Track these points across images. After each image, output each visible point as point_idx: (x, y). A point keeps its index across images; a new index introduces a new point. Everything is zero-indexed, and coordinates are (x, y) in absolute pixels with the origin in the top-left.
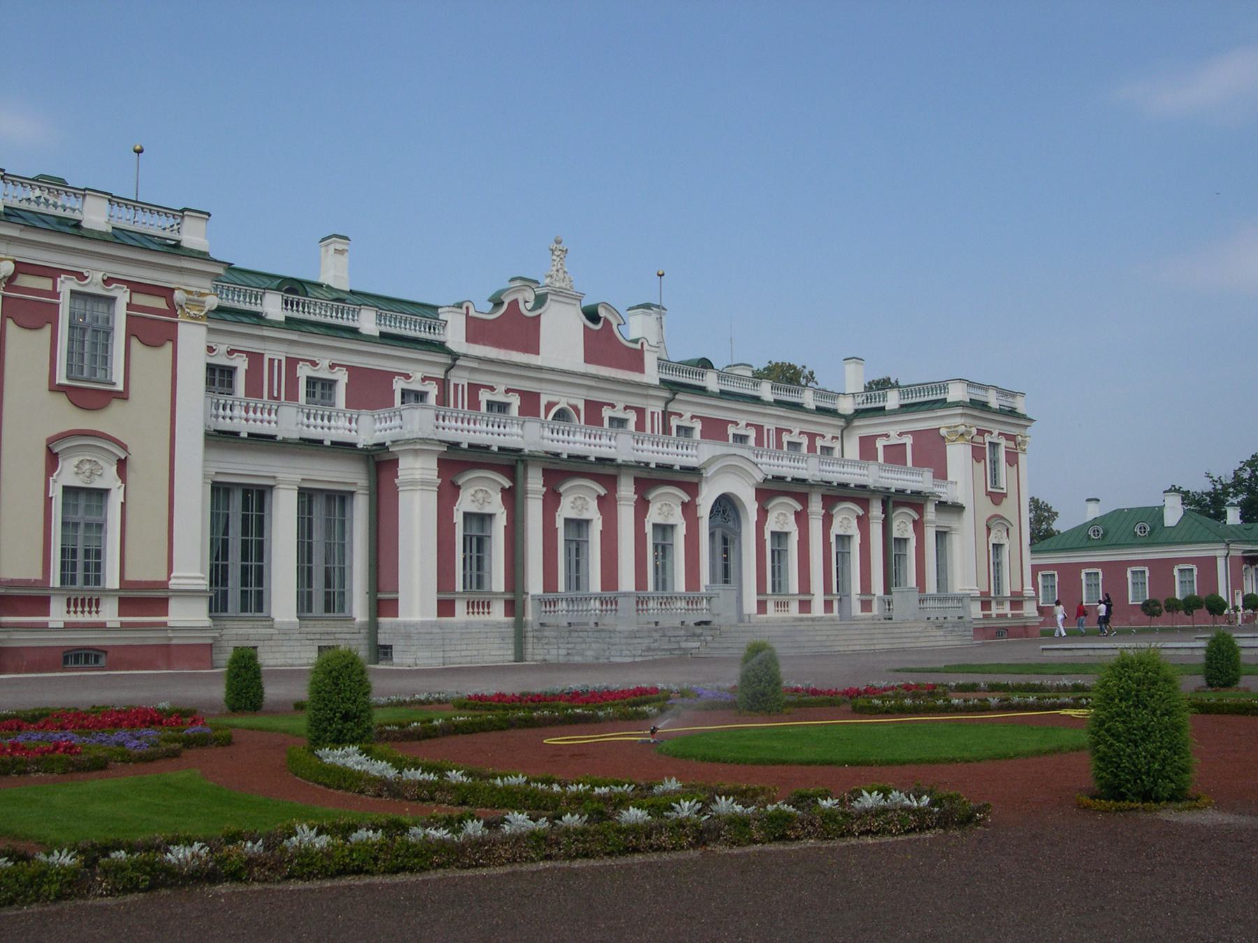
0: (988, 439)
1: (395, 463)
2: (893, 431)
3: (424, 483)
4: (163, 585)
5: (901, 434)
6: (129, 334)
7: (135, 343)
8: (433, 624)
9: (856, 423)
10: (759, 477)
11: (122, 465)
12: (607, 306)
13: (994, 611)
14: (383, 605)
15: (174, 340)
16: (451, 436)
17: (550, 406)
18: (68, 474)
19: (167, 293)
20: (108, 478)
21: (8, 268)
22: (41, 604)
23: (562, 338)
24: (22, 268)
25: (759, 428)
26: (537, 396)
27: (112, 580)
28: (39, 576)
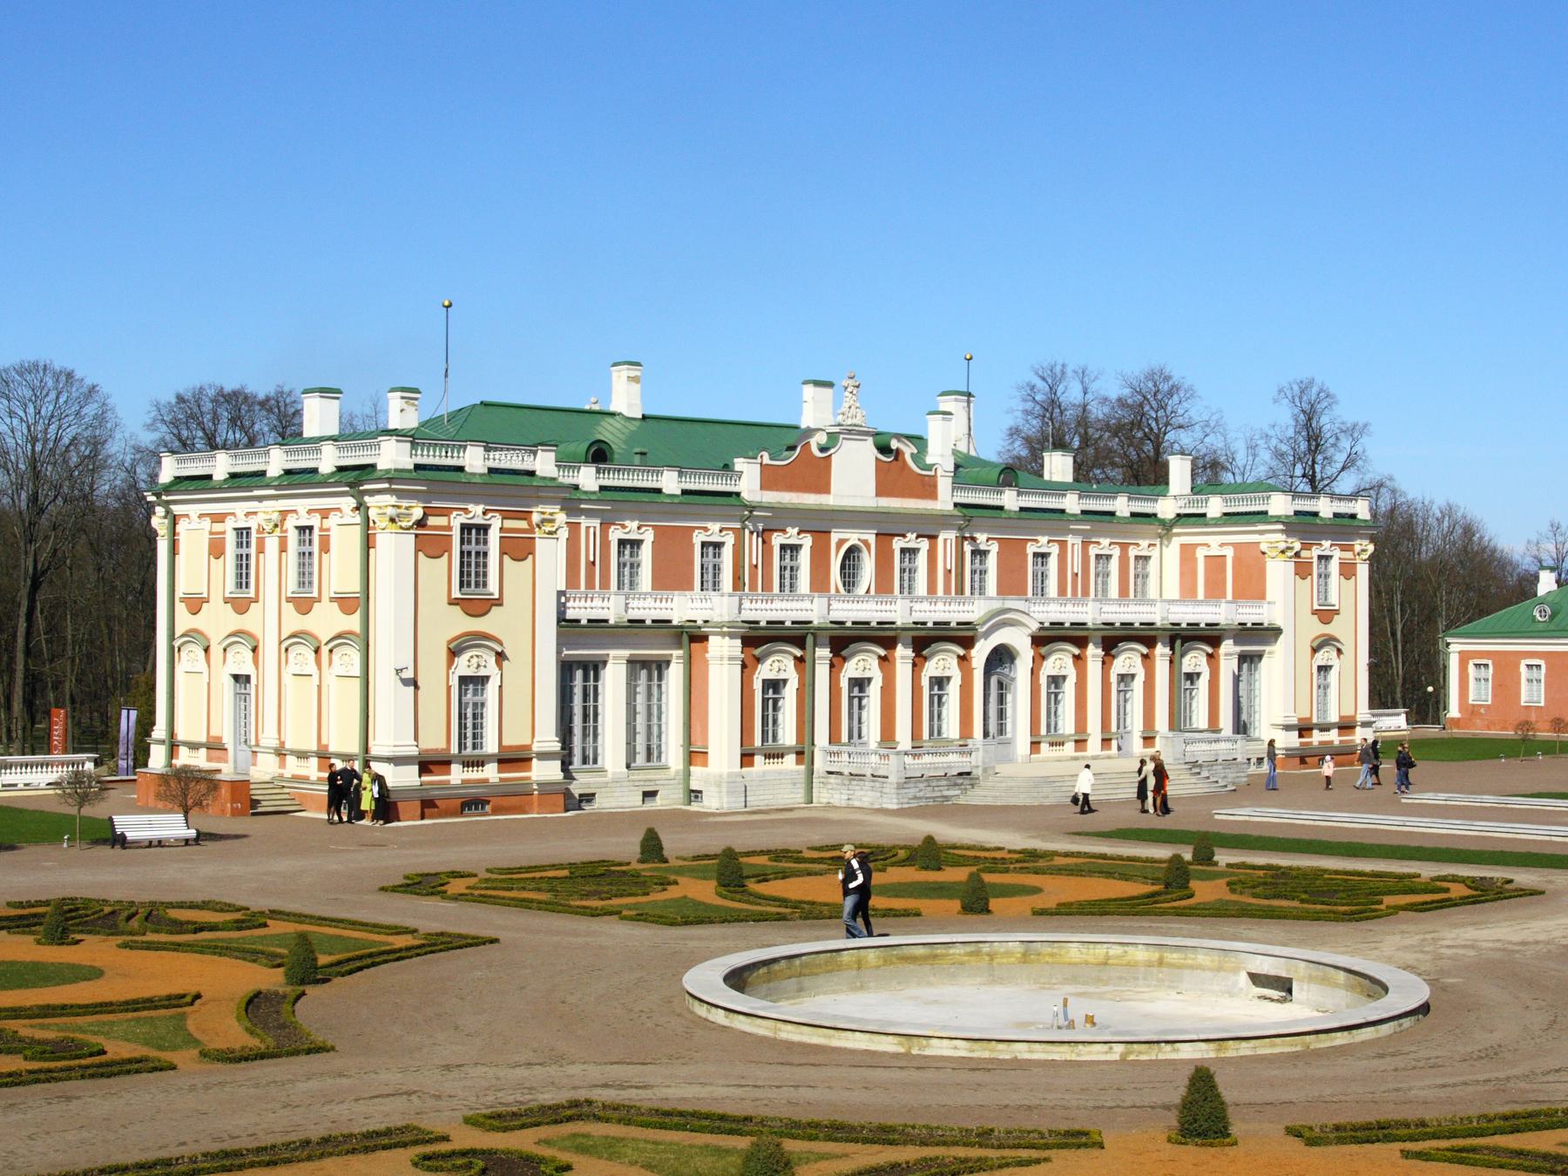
1: (704, 638)
2: (1214, 541)
3: (730, 659)
4: (528, 748)
5: (1222, 545)
6: (502, 553)
7: (506, 557)
8: (737, 775)
10: (1035, 626)
11: (501, 656)
14: (694, 755)
15: (532, 553)
16: (748, 615)
17: (841, 542)
28: (443, 745)
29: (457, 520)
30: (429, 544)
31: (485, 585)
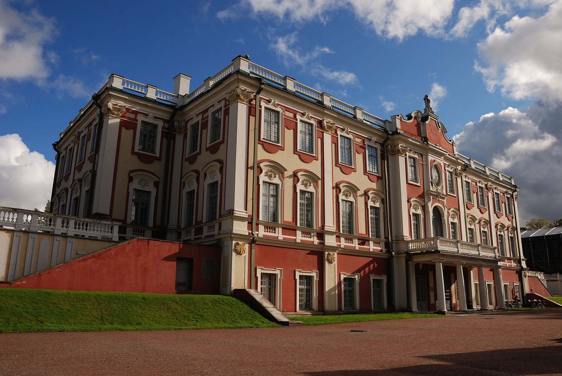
18: (135, 185)
27: (151, 224)
31: (153, 151)
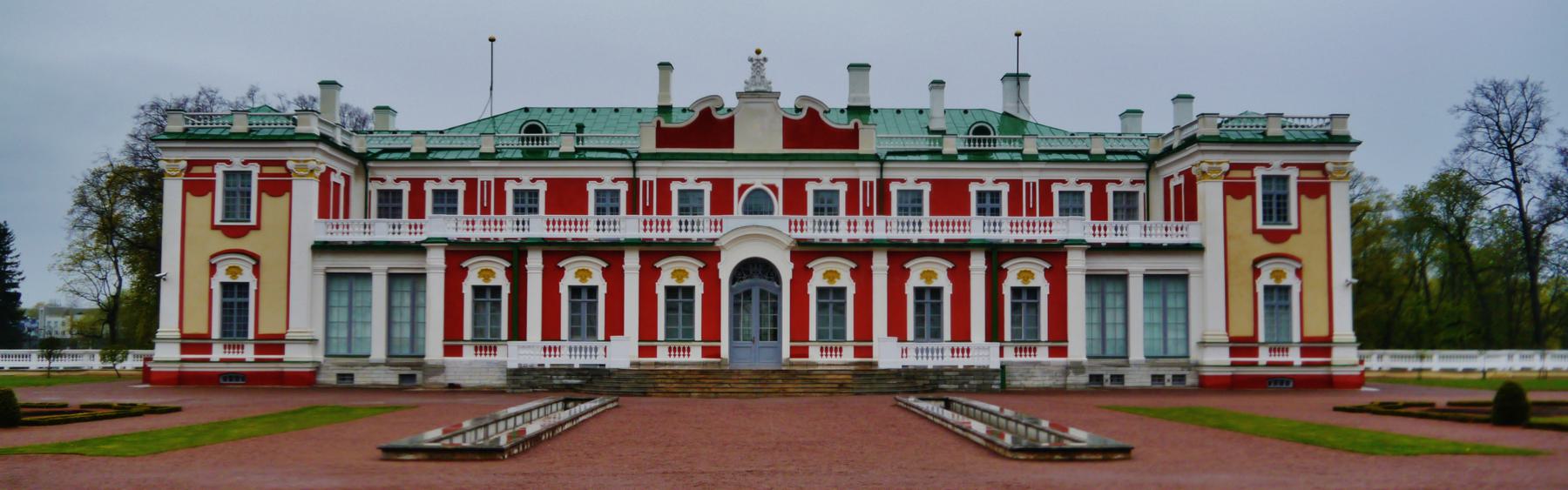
0: (1259, 173)
3: (437, 268)
7: (264, 196)
9: (1159, 164)
10: (788, 242)
11: (256, 270)
12: (804, 98)
13: (1264, 356)
17: (743, 188)
19: (282, 163)
20: (247, 276)
21: (184, 164)
22: (208, 349)
23: (759, 133)
24: (191, 163)
25: (1015, 185)
26: (730, 182)
27: (251, 335)
29: (220, 170)
30: (197, 186)
